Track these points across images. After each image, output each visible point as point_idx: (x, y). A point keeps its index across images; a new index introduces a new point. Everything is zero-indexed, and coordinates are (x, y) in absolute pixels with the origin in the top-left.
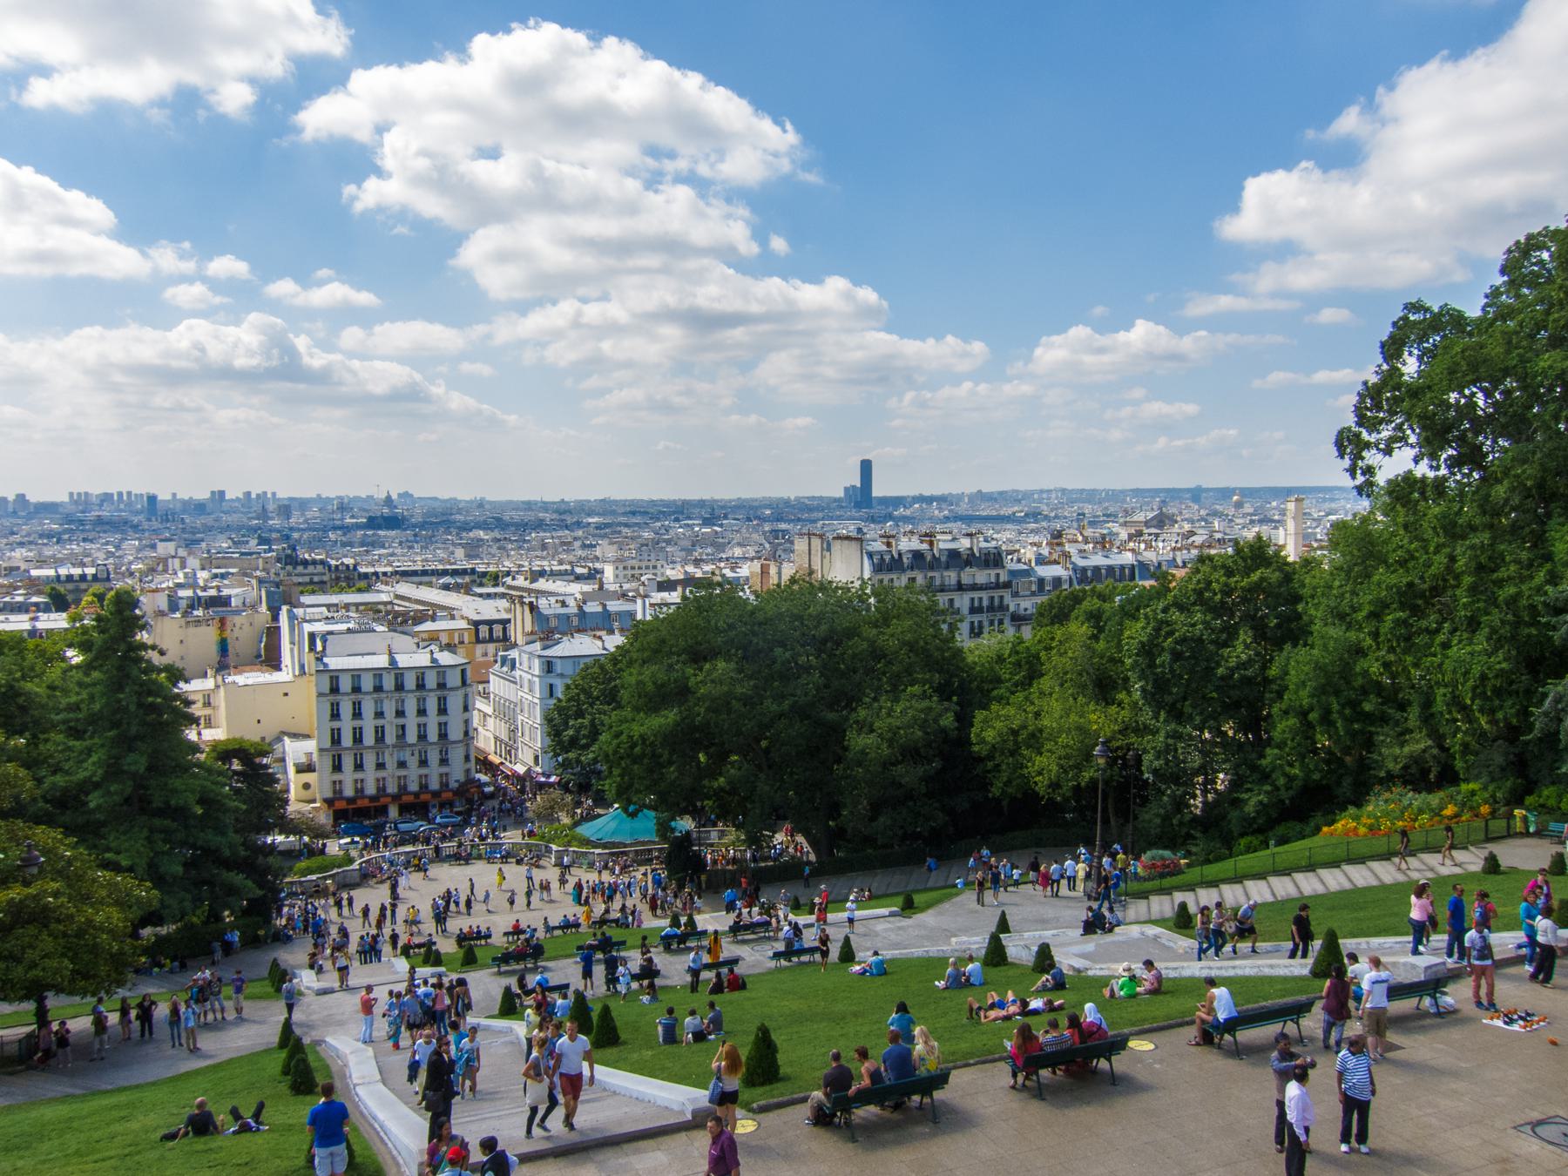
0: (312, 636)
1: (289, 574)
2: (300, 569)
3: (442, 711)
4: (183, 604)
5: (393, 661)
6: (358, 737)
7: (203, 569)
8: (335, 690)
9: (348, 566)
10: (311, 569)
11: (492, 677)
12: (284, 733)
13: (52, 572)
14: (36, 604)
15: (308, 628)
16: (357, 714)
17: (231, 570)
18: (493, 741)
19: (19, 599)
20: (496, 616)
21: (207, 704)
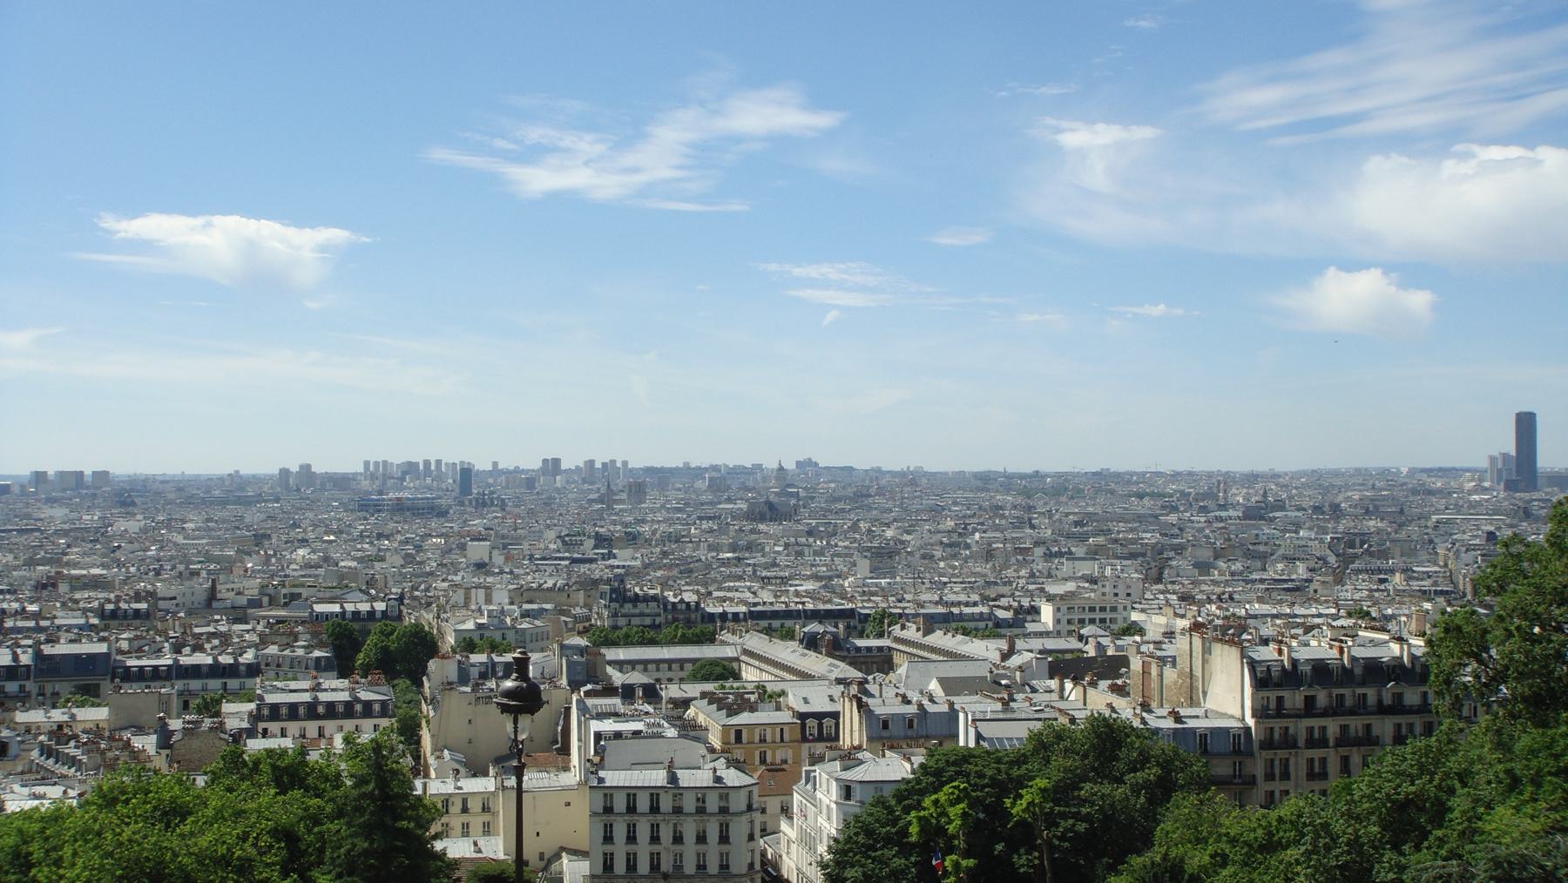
0: (598, 736)
1: (615, 615)
2: (628, 608)
3: (724, 839)
4: (474, 672)
5: (673, 779)
6: (631, 866)
7: (512, 603)
8: (608, 810)
9: (688, 604)
10: (642, 607)
11: (795, 794)
12: (563, 849)
13: (336, 608)
14: (318, 659)
15: (596, 726)
16: (631, 838)
17: (548, 606)
18: (795, 872)
19: (300, 652)
20: (828, 707)
21: (485, 809)
